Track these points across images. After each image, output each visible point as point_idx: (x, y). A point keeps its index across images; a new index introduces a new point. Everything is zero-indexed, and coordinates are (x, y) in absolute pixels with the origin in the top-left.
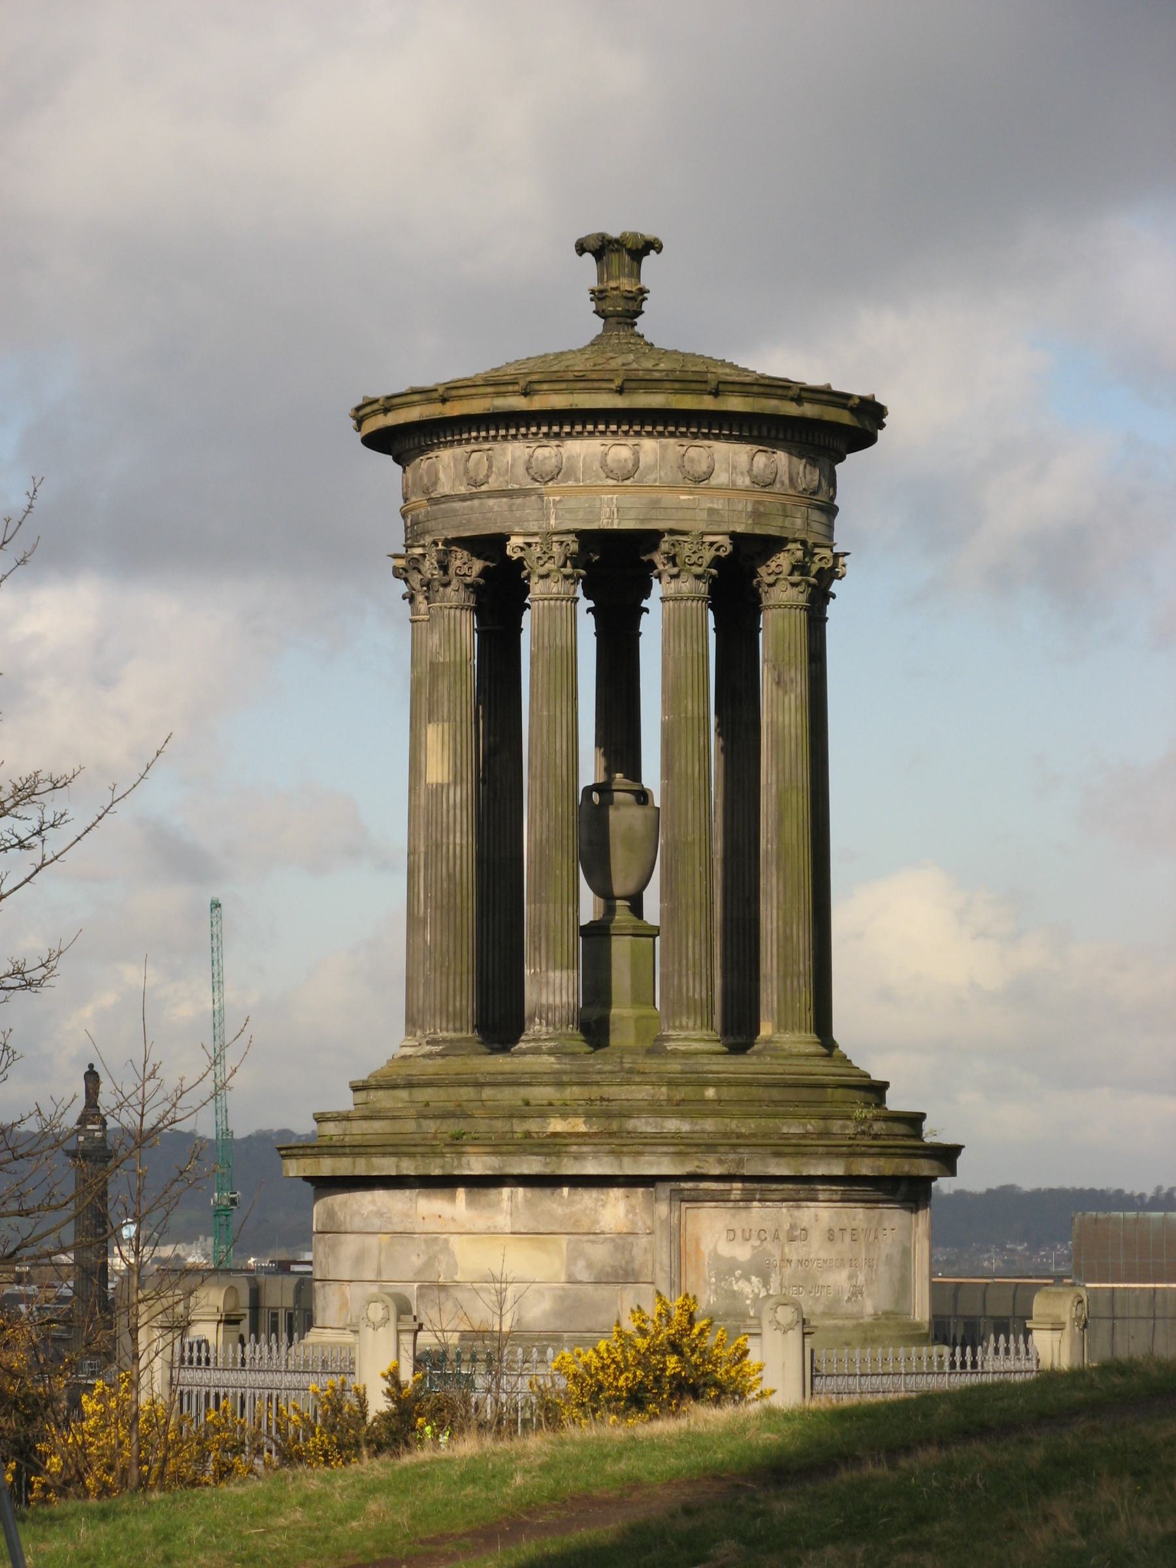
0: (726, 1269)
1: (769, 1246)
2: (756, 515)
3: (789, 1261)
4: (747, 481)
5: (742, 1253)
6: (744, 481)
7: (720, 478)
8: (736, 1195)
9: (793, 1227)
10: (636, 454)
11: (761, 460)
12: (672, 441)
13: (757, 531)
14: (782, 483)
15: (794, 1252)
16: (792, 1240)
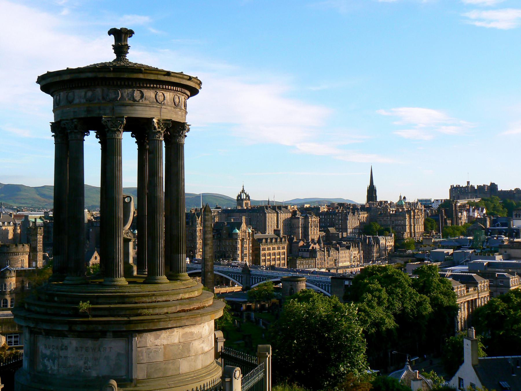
0: (44, 356)
1: (55, 351)
2: (88, 111)
3: (61, 357)
4: (85, 101)
5: (48, 352)
6: (83, 101)
7: (77, 101)
8: (44, 333)
9: (62, 345)
10: (60, 97)
11: (89, 94)
12: (65, 92)
13: (89, 116)
14: (99, 99)
15: (62, 353)
16: (62, 349)
